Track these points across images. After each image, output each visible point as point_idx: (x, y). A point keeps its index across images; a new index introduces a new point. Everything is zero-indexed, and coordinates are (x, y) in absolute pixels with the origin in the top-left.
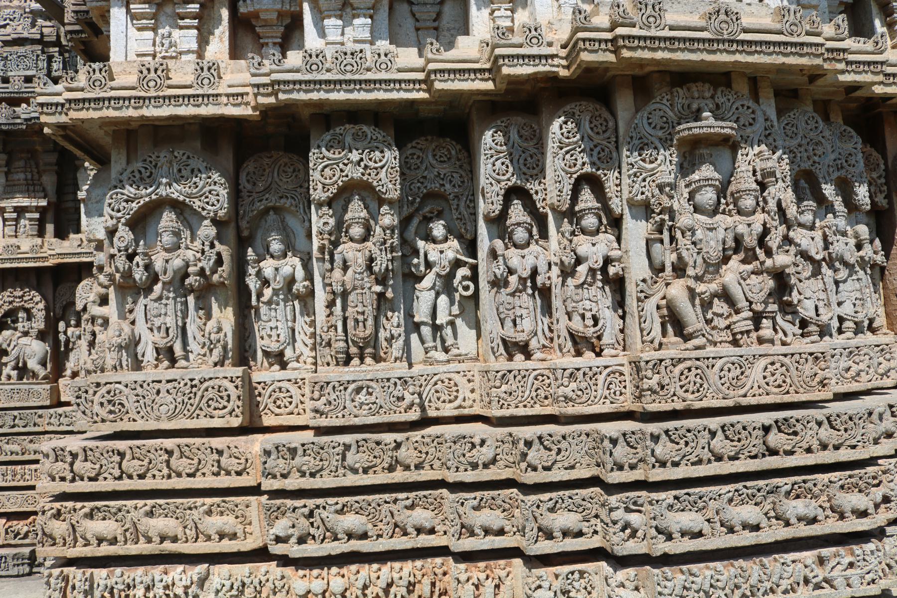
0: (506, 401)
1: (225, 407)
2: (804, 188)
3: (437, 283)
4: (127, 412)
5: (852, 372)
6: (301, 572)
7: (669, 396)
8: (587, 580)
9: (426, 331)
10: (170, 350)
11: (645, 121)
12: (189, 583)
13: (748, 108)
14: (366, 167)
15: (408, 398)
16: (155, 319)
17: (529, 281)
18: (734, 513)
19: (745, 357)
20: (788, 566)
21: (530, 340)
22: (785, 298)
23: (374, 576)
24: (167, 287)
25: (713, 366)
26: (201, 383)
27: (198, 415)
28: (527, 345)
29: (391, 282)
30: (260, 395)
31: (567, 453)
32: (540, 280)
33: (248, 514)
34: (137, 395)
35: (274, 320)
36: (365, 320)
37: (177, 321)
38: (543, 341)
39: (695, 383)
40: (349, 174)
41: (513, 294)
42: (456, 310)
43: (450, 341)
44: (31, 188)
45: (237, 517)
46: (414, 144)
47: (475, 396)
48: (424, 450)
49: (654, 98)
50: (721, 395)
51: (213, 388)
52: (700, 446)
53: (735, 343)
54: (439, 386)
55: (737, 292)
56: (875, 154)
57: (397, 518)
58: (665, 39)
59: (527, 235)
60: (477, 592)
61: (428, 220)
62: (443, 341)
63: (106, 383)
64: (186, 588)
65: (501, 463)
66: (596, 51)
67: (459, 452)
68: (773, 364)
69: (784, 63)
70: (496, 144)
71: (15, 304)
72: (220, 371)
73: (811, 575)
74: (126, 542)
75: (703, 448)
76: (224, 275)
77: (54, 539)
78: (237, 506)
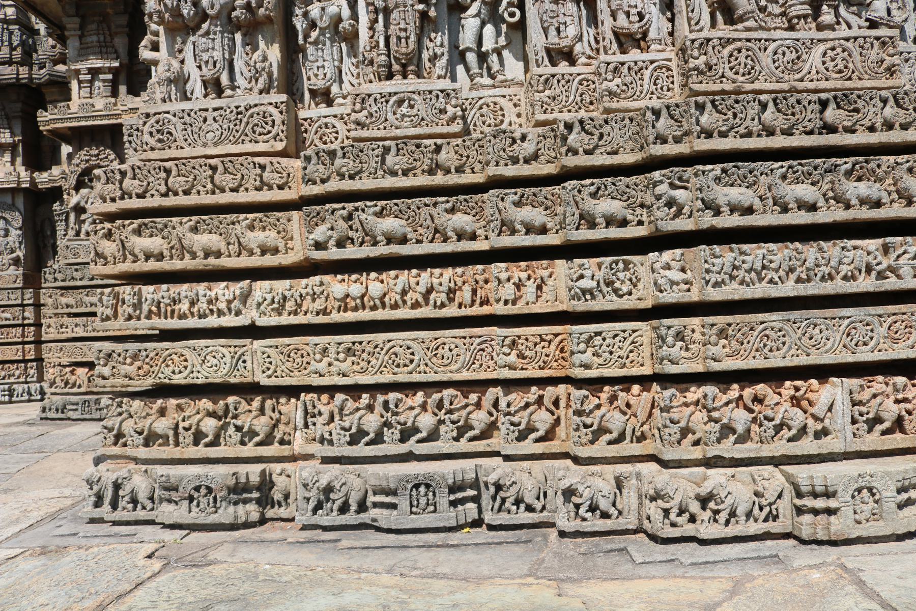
0: (549, 105)
1: (269, 132)
4: (175, 141)
6: (339, 277)
7: (717, 77)
8: (632, 271)
9: (471, 57)
10: (217, 82)
12: (231, 297)
15: (451, 110)
16: (203, 54)
20: (848, 251)
21: (574, 45)
23: (413, 281)
24: (214, 22)
25: (765, 49)
26: (247, 110)
27: (243, 140)
31: (610, 138)
33: (289, 228)
34: (185, 124)
35: (321, 60)
36: (407, 38)
37: (224, 54)
38: (589, 52)
39: (746, 65)
42: (502, 41)
43: (496, 67)
44: (104, 50)
45: (279, 233)
47: (522, 120)
48: (465, 154)
51: (258, 114)
52: (749, 117)
53: (791, 28)
60: (518, 293)
62: (489, 69)
63: (155, 114)
64: (229, 302)
65: (542, 158)
67: (499, 146)
68: (833, 49)
71: (91, 162)
72: (265, 98)
73: (874, 262)
74: (172, 258)
75: (753, 119)
76: (270, 6)
77: (106, 259)
78: (278, 220)
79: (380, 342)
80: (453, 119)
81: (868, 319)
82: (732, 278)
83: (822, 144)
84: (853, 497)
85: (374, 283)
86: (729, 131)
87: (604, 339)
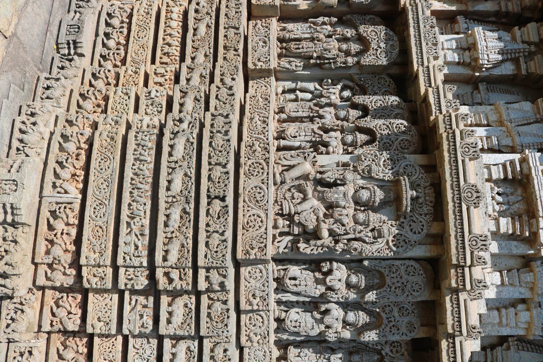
2: (373, 280)
3: (318, 92)
5: (251, 299)
9: (293, 85)
11: (408, 162)
14: (377, 50)
18: (179, 176)
19: (267, 204)
23: (175, 39)
25: (263, 183)
28: (282, 113)
29: (318, 62)
30: (266, 21)
32: (317, 119)
36: (299, 49)
41: (310, 108)
46: (392, 82)
52: (219, 158)
53: (276, 201)
54: (264, 87)
55: (306, 206)
57: (201, 49)
58: (456, 157)
59: (342, 117)
61: (351, 89)
66: (444, 123)
67: (230, 68)
68: (262, 221)
69: (450, 235)
79: (149, 25)
80: (255, 65)
81: (107, 215)
82: (138, 145)
84: (14, 181)
85: (176, 24)
87: (126, 100)
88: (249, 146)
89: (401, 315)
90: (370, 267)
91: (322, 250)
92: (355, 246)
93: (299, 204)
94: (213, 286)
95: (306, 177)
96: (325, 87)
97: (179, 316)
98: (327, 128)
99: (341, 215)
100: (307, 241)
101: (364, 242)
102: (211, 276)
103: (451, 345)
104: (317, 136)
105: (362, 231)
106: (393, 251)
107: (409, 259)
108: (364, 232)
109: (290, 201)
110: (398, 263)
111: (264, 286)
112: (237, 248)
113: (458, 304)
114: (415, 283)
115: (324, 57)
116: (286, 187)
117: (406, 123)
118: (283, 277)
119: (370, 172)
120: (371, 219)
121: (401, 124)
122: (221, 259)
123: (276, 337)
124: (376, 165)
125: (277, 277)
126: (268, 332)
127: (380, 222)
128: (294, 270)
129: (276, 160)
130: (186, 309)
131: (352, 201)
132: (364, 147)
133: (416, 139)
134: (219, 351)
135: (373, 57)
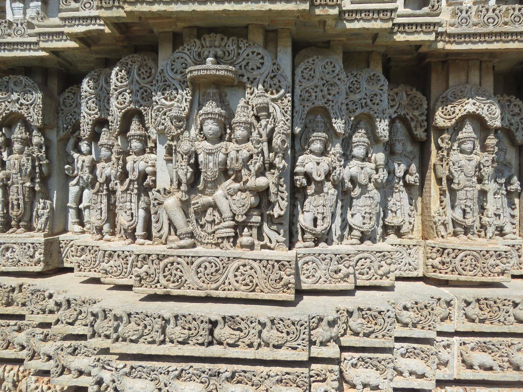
2: (318, 122)
11: (168, 68)
13: (258, 54)
14: (22, 104)
17: (105, 185)
19: (221, 258)
21: (102, 226)
22: (268, 212)
25: (192, 263)
28: (102, 229)
29: (38, 180)
32: (110, 186)
36: (18, 205)
39: (175, 275)
40: (11, 109)
46: (69, 89)
49: (178, 48)
50: (196, 286)
53: (217, 245)
55: (224, 205)
56: (419, 95)
66: (110, 8)
68: (244, 265)
69: (270, 10)
70: (90, 89)
80: (39, 262)
83: (208, 356)
86: (140, 337)
88: (140, 281)
89: (358, 91)
90: (302, 125)
91: (282, 186)
92: (279, 142)
93: (221, 215)
94: (333, 335)
95: (185, 205)
96: (76, 172)
97: (368, 375)
98: (121, 173)
99: (237, 160)
100: (271, 205)
101: (273, 130)
102: (321, 339)
103: (401, 29)
104: (131, 187)
105: (259, 133)
106: (285, 94)
107: (293, 75)
108: (261, 130)
109: (216, 227)
110: (298, 91)
111: (325, 259)
112: (281, 299)
113: (357, 11)
114: (324, 70)
115: (30, 173)
116: (198, 230)
117: (116, 69)
118: (314, 234)
119: (179, 119)
120: (244, 119)
121: (117, 75)
122: (298, 327)
123: (379, 241)
124: (171, 110)
125: (314, 242)
126: (377, 252)
127: (248, 108)
128: (304, 220)
129: (162, 243)
130: (359, 364)
131: (219, 145)
132: (147, 126)
133: (138, 57)
134: (406, 317)
135: (31, 110)
